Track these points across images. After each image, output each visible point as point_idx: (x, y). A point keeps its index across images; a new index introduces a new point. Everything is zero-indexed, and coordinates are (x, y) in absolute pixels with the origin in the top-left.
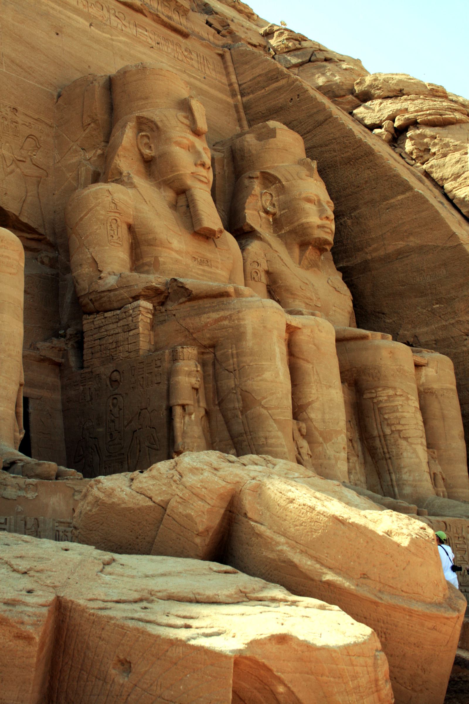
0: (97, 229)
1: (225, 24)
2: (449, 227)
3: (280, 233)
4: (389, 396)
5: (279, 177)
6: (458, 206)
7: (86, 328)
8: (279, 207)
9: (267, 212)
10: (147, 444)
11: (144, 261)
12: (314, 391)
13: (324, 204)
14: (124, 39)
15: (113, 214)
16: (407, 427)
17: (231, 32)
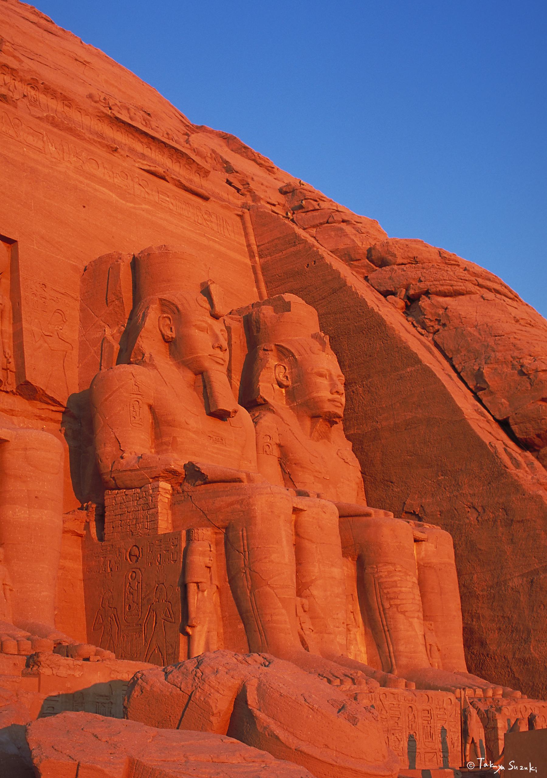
0: (120, 410)
1: (245, 183)
2: (454, 401)
3: (292, 405)
4: (388, 571)
5: (293, 351)
6: (465, 379)
7: (107, 503)
8: (292, 380)
10: (163, 616)
11: (163, 441)
12: (316, 570)
13: (335, 378)
15: (135, 396)
16: (404, 602)
17: (250, 191)
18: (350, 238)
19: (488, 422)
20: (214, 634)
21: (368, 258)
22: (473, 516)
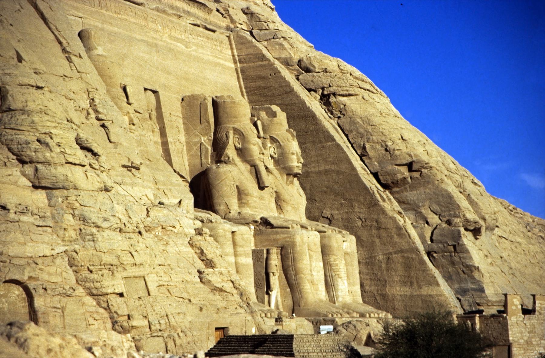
5: (279, 140)
6: (356, 148)
9: (272, 157)
14: (194, 48)
17: (229, 16)
18: (288, 52)
19: (368, 174)
20: (279, 293)
21: (298, 65)
22: (359, 223)
